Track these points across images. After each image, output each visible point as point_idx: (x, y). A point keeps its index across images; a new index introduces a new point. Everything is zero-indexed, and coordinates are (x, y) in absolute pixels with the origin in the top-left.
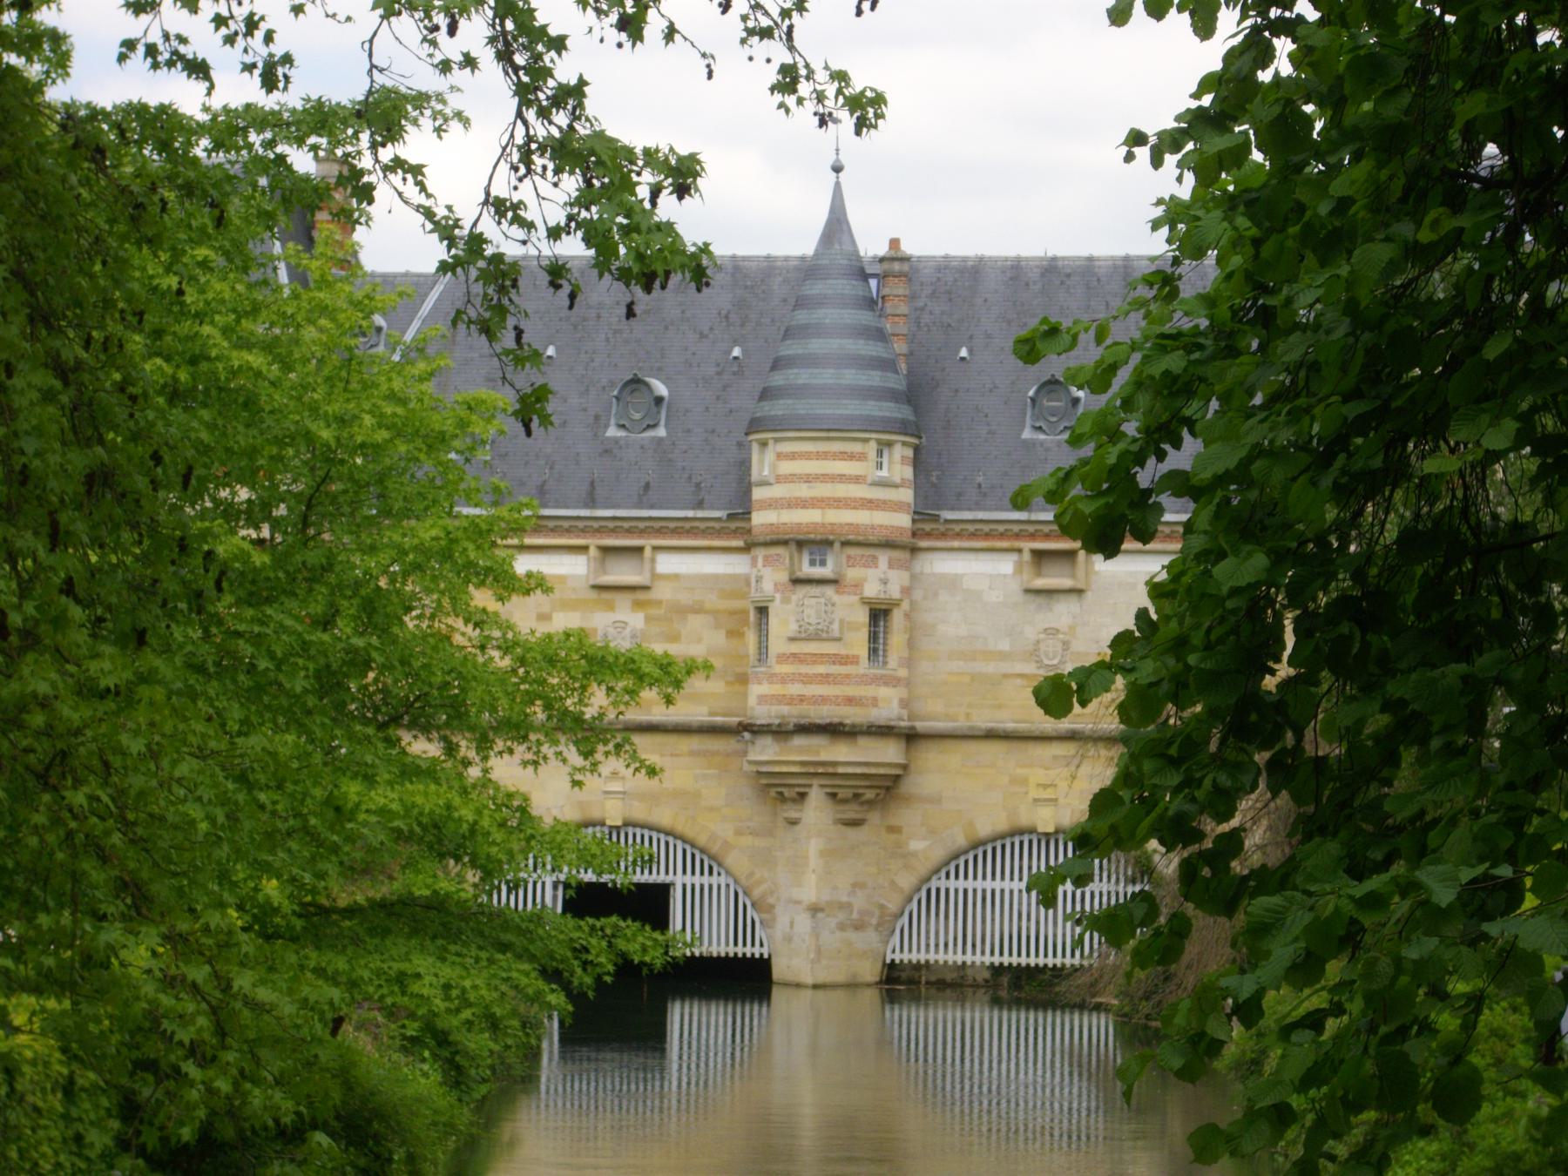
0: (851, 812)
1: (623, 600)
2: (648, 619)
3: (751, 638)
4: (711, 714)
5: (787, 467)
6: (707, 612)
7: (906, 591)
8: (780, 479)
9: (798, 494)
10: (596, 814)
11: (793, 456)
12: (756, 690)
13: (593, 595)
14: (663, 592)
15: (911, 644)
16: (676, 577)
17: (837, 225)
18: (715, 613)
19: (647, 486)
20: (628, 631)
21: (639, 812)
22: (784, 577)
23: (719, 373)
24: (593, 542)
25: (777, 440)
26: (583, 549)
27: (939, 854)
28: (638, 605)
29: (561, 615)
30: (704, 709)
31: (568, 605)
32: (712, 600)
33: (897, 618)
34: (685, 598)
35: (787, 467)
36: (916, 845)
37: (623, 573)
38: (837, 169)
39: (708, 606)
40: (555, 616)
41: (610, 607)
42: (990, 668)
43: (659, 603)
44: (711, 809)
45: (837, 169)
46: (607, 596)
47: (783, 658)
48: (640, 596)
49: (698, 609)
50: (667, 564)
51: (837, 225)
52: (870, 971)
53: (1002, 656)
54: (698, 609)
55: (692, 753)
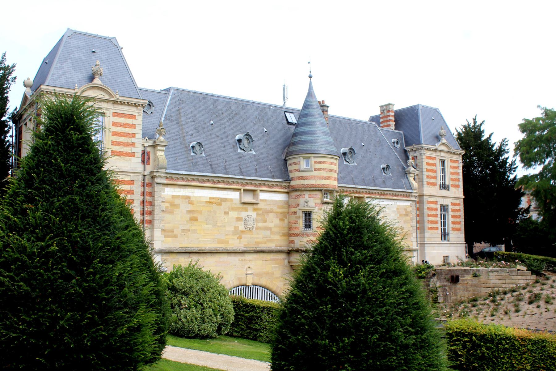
1: (250, 207)
2: (258, 214)
4: (276, 246)
5: (318, 166)
6: (274, 213)
8: (315, 170)
9: (323, 175)
10: (244, 282)
11: (321, 162)
13: (241, 206)
14: (261, 206)
16: (265, 200)
17: (310, 94)
18: (276, 213)
19: (256, 169)
20: (252, 219)
21: (257, 281)
22: (319, 201)
23: (263, 136)
24: (242, 188)
25: (314, 157)
28: (255, 210)
29: (232, 212)
30: (274, 245)
31: (233, 209)
32: (275, 209)
34: (268, 208)
35: (318, 166)
37: (248, 198)
38: (310, 77)
39: (274, 210)
40: (229, 212)
41: (246, 210)
43: (261, 209)
44: (277, 278)
45: (310, 77)
46: (246, 206)
48: (255, 206)
49: (271, 212)
50: (263, 196)
51: (310, 94)
54: (271, 212)
55: (271, 260)
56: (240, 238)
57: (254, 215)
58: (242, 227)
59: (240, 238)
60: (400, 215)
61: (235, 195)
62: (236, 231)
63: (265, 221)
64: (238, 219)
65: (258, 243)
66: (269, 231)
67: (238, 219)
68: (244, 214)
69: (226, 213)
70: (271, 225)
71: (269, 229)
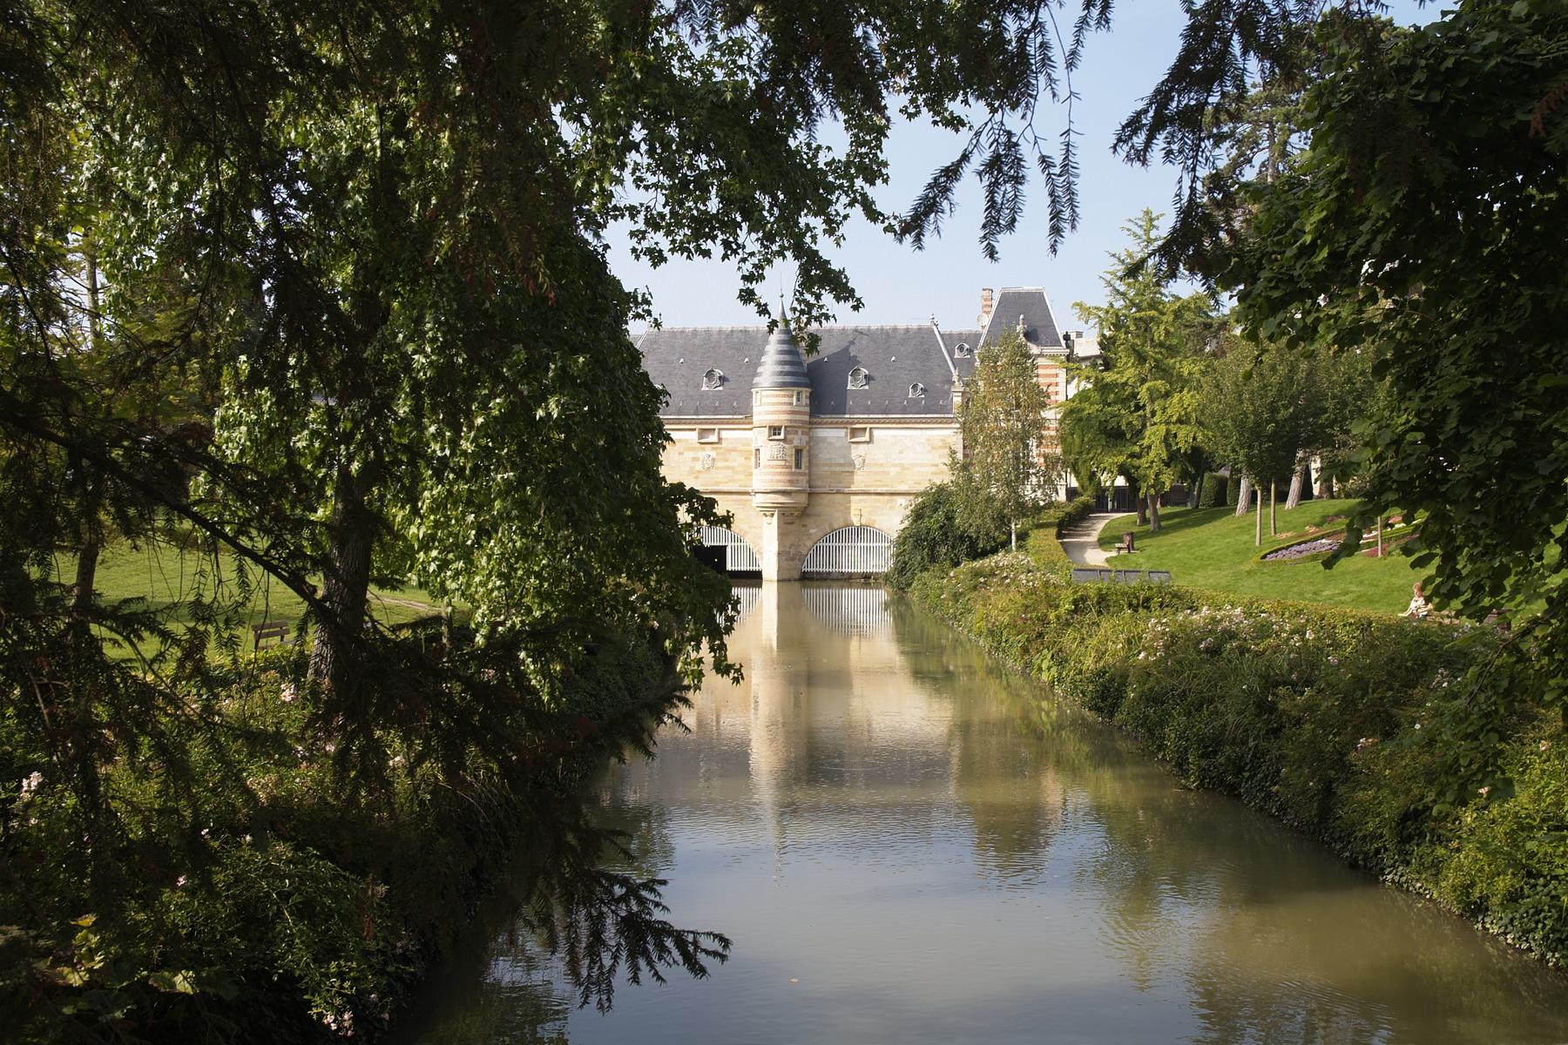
0: (790, 519)
3: (753, 459)
7: (808, 443)
12: (755, 478)
14: (724, 444)
15: (810, 461)
26: (694, 430)
27: (820, 534)
32: (740, 447)
33: (805, 453)
34: (730, 446)
36: (812, 531)
41: (704, 449)
42: (837, 469)
47: (765, 467)
50: (724, 434)
52: (796, 575)
53: (842, 465)
56: (697, 477)
57: (713, 454)
58: (699, 467)
59: (697, 477)
60: (933, 448)
61: (694, 435)
62: (691, 471)
63: (727, 460)
64: (695, 459)
65: (717, 483)
66: (730, 472)
67: (695, 459)
68: (701, 454)
69: (681, 454)
70: (733, 464)
71: (733, 468)
